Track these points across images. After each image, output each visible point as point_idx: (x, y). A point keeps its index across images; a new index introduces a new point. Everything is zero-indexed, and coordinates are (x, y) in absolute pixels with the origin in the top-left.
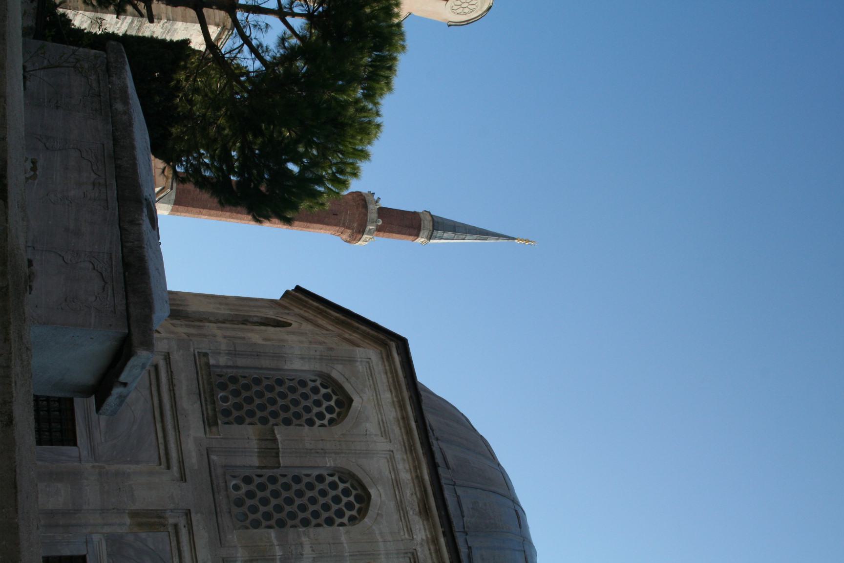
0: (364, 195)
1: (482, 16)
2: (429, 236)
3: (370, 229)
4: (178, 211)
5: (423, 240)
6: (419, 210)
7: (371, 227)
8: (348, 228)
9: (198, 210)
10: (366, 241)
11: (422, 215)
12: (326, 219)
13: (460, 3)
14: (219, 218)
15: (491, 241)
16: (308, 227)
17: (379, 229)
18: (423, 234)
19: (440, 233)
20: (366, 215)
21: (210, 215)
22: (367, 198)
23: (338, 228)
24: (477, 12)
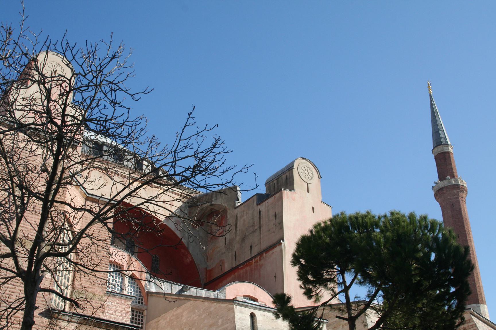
0: (435, 192)
1: (309, 161)
2: (447, 145)
3: (455, 182)
4: (482, 300)
5: (450, 148)
6: (433, 157)
7: (453, 182)
8: (458, 195)
9: (477, 288)
10: (463, 181)
11: (436, 154)
12: (457, 209)
13: (307, 176)
14: (479, 274)
15: (437, 108)
16: (466, 219)
17: (453, 176)
18: (446, 149)
19: (443, 140)
20: (447, 187)
21: (478, 280)
22: (437, 189)
23: (460, 201)
24: (308, 165)
